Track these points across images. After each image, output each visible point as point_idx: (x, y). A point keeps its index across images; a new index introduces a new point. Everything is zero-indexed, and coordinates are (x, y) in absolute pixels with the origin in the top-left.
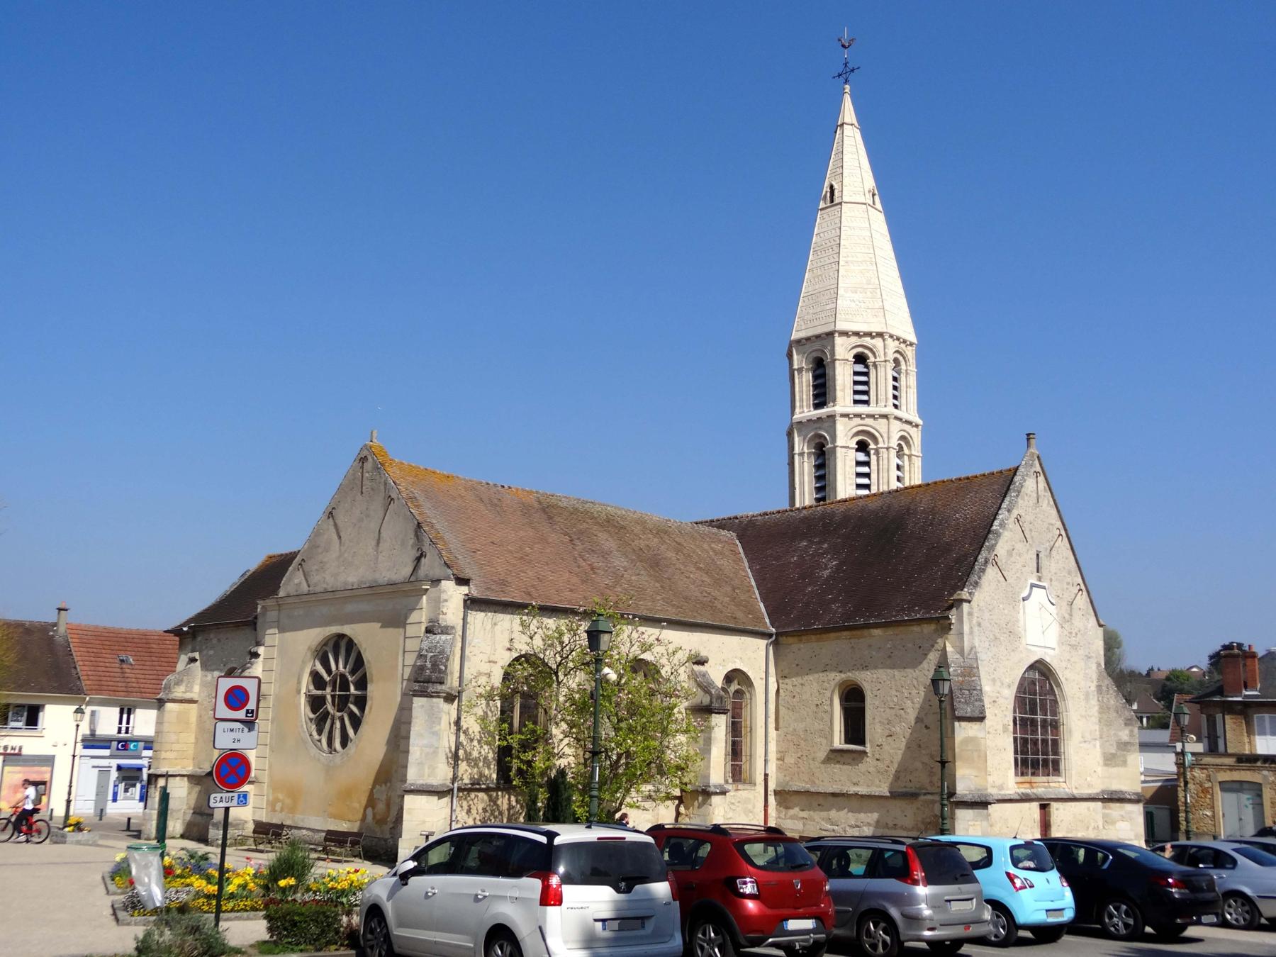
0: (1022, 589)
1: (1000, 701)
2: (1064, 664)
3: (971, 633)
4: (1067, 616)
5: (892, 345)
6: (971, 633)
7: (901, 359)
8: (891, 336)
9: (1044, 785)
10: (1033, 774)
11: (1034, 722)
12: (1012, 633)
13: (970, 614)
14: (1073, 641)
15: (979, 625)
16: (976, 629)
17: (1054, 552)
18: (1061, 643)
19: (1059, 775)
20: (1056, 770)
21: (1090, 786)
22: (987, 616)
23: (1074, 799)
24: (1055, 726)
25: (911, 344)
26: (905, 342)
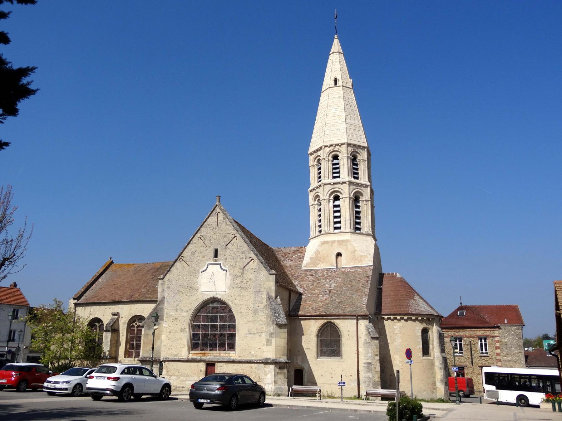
0: (201, 267)
1: (180, 319)
2: (234, 298)
3: (163, 291)
4: (239, 274)
5: (328, 150)
6: (163, 291)
7: (336, 153)
8: (326, 146)
9: (212, 355)
10: (210, 350)
11: (214, 327)
12: (192, 288)
13: (163, 284)
14: (244, 285)
15: (169, 287)
16: (166, 290)
17: (229, 246)
18: (232, 287)
19: (234, 350)
20: (232, 347)
21: (253, 356)
22: (174, 283)
23: (234, 362)
24: (233, 327)
25: (343, 144)
26: (337, 145)
